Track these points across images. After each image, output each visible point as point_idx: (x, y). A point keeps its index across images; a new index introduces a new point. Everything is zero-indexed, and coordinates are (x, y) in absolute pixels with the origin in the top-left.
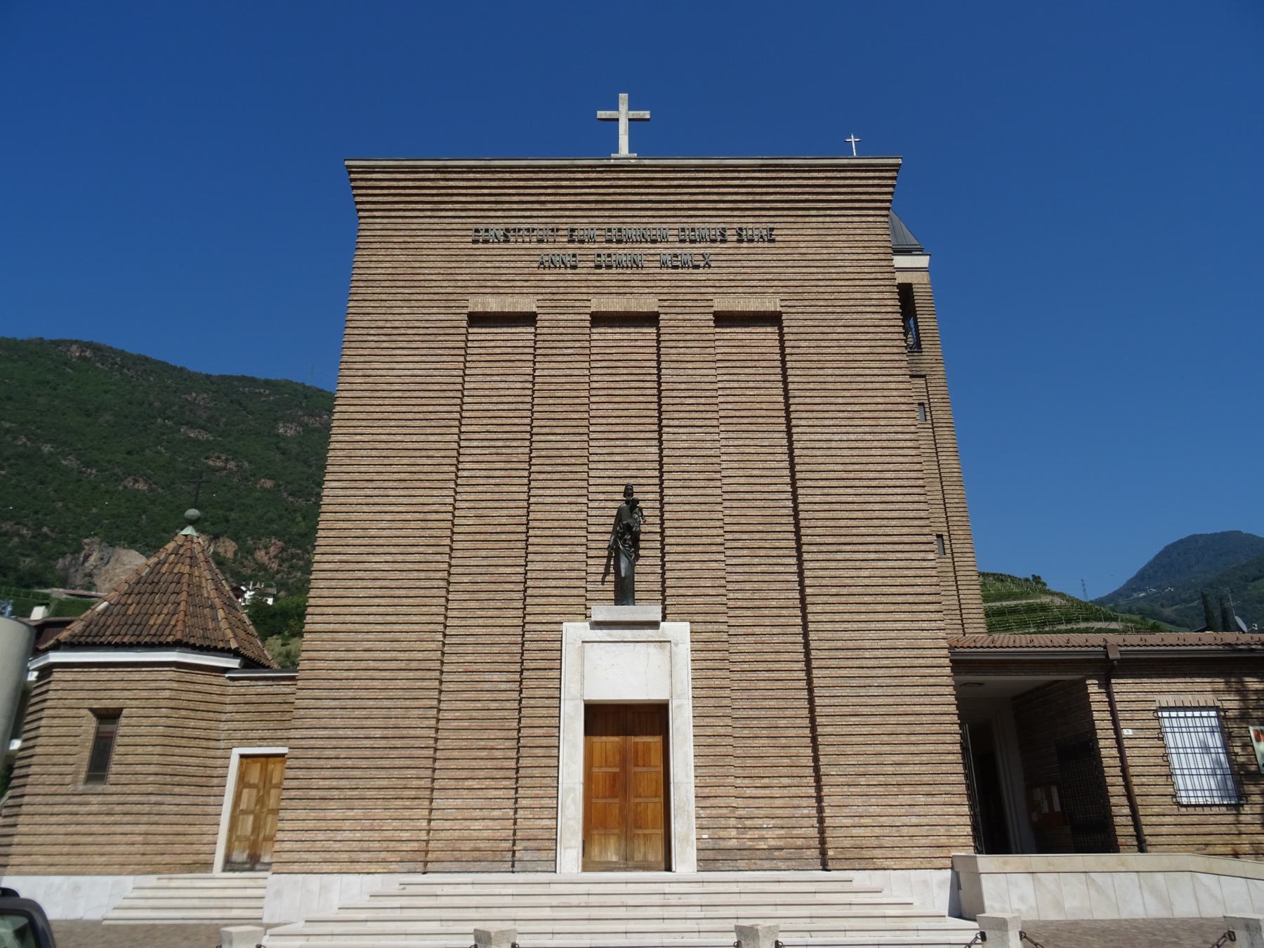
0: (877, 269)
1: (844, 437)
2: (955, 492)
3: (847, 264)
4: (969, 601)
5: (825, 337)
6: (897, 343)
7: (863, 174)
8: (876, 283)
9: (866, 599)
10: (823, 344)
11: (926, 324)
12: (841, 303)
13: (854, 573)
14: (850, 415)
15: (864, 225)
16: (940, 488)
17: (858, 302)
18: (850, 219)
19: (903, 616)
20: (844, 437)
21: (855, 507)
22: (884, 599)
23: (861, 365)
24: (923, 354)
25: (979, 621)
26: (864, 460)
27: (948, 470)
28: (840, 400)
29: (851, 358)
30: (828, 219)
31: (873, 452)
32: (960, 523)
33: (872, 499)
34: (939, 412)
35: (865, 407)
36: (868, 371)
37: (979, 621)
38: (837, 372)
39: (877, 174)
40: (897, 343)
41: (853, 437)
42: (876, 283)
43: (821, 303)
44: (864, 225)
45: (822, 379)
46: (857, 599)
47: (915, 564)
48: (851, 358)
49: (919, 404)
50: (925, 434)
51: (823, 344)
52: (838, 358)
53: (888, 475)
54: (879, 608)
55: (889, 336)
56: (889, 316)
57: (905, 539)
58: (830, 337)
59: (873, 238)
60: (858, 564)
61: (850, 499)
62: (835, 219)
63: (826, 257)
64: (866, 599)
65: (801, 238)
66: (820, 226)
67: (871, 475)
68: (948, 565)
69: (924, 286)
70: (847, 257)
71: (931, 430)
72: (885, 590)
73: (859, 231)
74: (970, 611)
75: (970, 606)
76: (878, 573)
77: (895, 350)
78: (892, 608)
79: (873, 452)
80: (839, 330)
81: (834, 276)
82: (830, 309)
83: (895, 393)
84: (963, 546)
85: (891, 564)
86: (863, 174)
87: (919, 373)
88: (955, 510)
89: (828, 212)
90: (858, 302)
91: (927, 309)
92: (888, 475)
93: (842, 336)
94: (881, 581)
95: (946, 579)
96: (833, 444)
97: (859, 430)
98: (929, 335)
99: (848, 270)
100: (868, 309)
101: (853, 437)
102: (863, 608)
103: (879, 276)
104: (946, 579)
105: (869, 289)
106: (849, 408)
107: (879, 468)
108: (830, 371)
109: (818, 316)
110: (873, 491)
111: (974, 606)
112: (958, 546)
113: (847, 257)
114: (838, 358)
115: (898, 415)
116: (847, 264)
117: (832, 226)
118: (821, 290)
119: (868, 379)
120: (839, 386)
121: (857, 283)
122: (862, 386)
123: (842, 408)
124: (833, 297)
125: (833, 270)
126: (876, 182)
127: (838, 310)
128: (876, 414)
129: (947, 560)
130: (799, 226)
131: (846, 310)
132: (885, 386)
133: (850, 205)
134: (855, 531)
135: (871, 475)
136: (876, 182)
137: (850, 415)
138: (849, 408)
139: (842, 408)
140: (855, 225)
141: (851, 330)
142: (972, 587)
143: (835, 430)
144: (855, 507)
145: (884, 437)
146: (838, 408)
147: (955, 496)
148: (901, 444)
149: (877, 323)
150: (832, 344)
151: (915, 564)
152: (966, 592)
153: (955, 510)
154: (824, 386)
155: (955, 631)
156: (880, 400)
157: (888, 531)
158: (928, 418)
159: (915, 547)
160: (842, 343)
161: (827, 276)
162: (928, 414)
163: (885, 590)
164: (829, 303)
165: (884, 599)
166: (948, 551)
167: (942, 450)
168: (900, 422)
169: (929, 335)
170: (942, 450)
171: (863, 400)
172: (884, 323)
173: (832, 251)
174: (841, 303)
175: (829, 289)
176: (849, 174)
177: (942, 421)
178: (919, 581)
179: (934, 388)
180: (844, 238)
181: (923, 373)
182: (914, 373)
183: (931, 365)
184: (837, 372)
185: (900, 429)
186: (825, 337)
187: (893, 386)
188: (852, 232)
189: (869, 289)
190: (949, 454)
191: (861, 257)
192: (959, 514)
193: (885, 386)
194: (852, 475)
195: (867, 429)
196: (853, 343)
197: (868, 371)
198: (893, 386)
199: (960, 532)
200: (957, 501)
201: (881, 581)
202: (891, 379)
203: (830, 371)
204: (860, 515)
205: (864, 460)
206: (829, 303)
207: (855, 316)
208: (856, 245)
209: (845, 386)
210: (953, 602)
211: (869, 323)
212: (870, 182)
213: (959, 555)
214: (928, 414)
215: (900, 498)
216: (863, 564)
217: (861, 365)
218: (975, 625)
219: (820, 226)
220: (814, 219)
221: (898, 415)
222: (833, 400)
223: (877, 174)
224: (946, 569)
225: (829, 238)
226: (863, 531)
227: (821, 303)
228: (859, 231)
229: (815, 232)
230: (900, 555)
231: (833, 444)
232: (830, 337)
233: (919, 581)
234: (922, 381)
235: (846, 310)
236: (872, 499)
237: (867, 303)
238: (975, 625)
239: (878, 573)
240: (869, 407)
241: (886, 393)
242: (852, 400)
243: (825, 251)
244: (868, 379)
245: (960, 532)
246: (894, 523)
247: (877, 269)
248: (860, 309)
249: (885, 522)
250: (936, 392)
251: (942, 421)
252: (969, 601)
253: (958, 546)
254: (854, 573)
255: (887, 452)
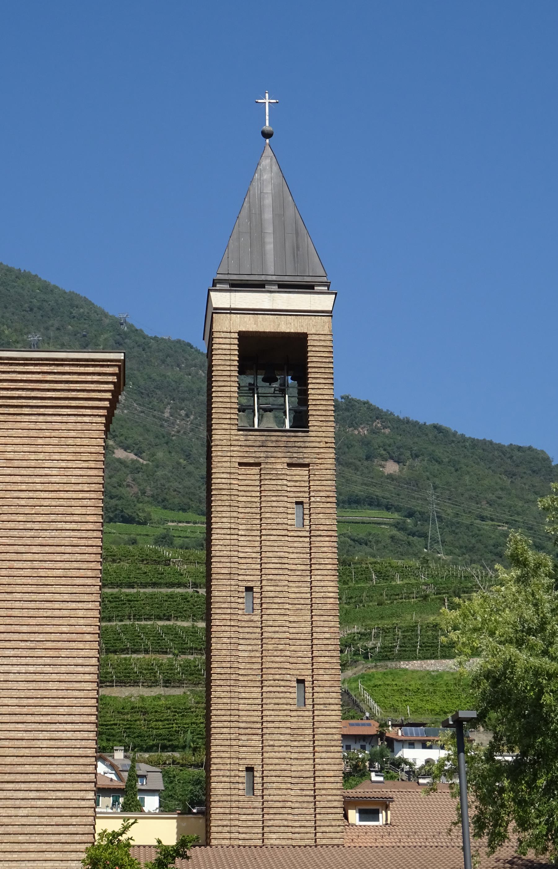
0: (85, 480)
1: (23, 669)
2: (326, 624)
3: (55, 472)
4: (326, 767)
5: (19, 557)
6: (92, 565)
7: (82, 369)
8: (81, 495)
9: (21, 838)
10: (16, 565)
11: (319, 392)
12: (41, 518)
13: (12, 812)
14: (32, 645)
15: (79, 426)
16: (309, 618)
17: (59, 518)
18: (65, 419)
19: (54, 856)
20: (23, 669)
21: (24, 743)
22: (38, 838)
23: (52, 589)
24: (311, 434)
25: (335, 792)
26: (40, 694)
27: (322, 595)
28: (25, 629)
29: (43, 581)
30: (41, 418)
31: (50, 685)
32: (327, 666)
33: (41, 735)
34: (321, 516)
35: (48, 637)
36: (57, 597)
37: (335, 792)
38: (27, 597)
39: (98, 369)
40: (92, 565)
41: (31, 669)
42: (81, 495)
43: (21, 518)
44: (79, 426)
45: (9, 605)
46: (12, 838)
47: (75, 803)
48: (43, 581)
49: (297, 503)
50: (300, 545)
51: (16, 565)
52: (30, 581)
53: (62, 710)
54: (32, 847)
55: (86, 557)
56: (89, 534)
57: (68, 777)
58: (25, 557)
59: (86, 442)
60: (18, 803)
61: (20, 735)
62: (49, 419)
63: (33, 464)
64: (21, 838)
65: (9, 441)
66: (32, 426)
67: (45, 710)
68: (306, 719)
69: (322, 338)
70: (55, 464)
71: (308, 539)
72: (41, 829)
73: (72, 434)
74: (327, 779)
75: (326, 773)
76: (36, 812)
77: (89, 573)
78: (44, 847)
79: (50, 685)
80: (35, 549)
81: (39, 487)
82: (29, 525)
83: (82, 621)
84: (327, 695)
85: (50, 803)
86: (82, 369)
87: (301, 461)
88: (323, 648)
89: (42, 411)
90: (59, 518)
91: (323, 370)
92: (62, 710)
93: (37, 557)
94: (37, 820)
95: (301, 738)
96: (11, 677)
97: (40, 661)
98: (320, 408)
99: (53, 479)
100: (68, 526)
101: (31, 669)
102: (17, 847)
103: (86, 487)
104: (301, 738)
105: (73, 503)
106: (32, 637)
107: (54, 702)
108: (19, 596)
109: (15, 533)
110: (44, 727)
111: (332, 773)
112: (321, 695)
113: (55, 464)
114: (30, 581)
115: (81, 645)
116: (55, 472)
117: (44, 426)
118: (23, 502)
119: (57, 605)
120: (25, 613)
121: (62, 495)
122: (49, 613)
123: (25, 637)
124: (33, 512)
125: (37, 480)
126: (96, 378)
127: (37, 526)
128: (59, 645)
129: (307, 713)
130: (9, 425)
131: (45, 526)
132: (72, 613)
133: (66, 403)
134: (19, 769)
135: (45, 710)
136: (96, 378)
137: (32, 645)
138: (32, 637)
139: (25, 637)
140: (70, 426)
141: (47, 549)
142: (332, 749)
143: (14, 661)
144: (24, 743)
145: (63, 669)
146: (21, 637)
147: (326, 629)
148: (80, 677)
149: (75, 541)
150: (25, 565)
151: (75, 803)
152: (324, 755)
153: (323, 648)
154: (10, 612)
155: (305, 805)
156: (65, 629)
157: (52, 769)
158: (307, 522)
159: (77, 786)
160: (36, 564)
161: (31, 487)
162: (307, 517)
163: (41, 829)
164: (29, 518)
165: (38, 838)
166: (309, 702)
167: (317, 567)
168: (82, 653)
169: (320, 408)
170: (317, 567)
171: (48, 629)
172: (83, 542)
173: (41, 456)
174: (41, 518)
175: (31, 502)
176: (67, 369)
177: (322, 527)
178: (74, 821)
179: (318, 483)
180: (55, 441)
181: (307, 461)
182: (294, 461)
183: (317, 450)
184: (27, 597)
185: (80, 661)
186: (19, 557)
187: (81, 613)
188: (65, 434)
189: (73, 503)
190: (325, 572)
191: (70, 464)
192: (328, 654)
193: (72, 613)
194: (25, 710)
195: (48, 661)
196: (46, 565)
197: (57, 597)
198: (81, 613)
199: (326, 677)
200: (327, 636)
201: (37, 820)
202: (80, 605)
203: (19, 596)
204: (27, 752)
205: (40, 694)
206: (29, 518)
207: (54, 533)
208: (66, 450)
209: (32, 613)
210: (307, 767)
211: (66, 542)
212: (89, 378)
213: (322, 707)
214: (307, 517)
215: (69, 735)
216: (23, 803)
217: (52, 589)
218: (330, 798)
219: (32, 426)
220: (26, 418)
221: (81, 645)
222: (17, 628)
223: (98, 369)
224: (303, 725)
225: (40, 441)
226: (28, 768)
227: (21, 518)
228: (72, 434)
229: (25, 433)
230: (59, 794)
231: (11, 677)
232: (25, 557)
233: (74, 821)
234: (304, 472)
235: (45, 526)
236: (41, 735)
237: (68, 518)
238: (330, 798)
239: (36, 812)
240: (52, 637)
241: (73, 621)
242: (36, 629)
243: (33, 457)
244: (57, 605)
245: (326, 677)
246: (59, 760)
247: (85, 480)
248: (60, 526)
249: (51, 760)
250: (319, 488)
251: (322, 527)
252: (326, 767)
253: (321, 695)
254: (12, 812)
255: (63, 686)
